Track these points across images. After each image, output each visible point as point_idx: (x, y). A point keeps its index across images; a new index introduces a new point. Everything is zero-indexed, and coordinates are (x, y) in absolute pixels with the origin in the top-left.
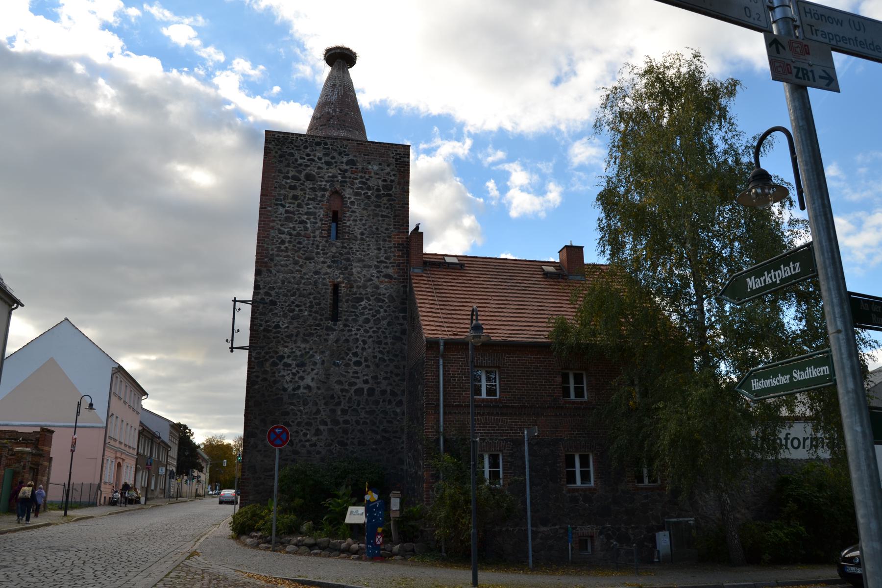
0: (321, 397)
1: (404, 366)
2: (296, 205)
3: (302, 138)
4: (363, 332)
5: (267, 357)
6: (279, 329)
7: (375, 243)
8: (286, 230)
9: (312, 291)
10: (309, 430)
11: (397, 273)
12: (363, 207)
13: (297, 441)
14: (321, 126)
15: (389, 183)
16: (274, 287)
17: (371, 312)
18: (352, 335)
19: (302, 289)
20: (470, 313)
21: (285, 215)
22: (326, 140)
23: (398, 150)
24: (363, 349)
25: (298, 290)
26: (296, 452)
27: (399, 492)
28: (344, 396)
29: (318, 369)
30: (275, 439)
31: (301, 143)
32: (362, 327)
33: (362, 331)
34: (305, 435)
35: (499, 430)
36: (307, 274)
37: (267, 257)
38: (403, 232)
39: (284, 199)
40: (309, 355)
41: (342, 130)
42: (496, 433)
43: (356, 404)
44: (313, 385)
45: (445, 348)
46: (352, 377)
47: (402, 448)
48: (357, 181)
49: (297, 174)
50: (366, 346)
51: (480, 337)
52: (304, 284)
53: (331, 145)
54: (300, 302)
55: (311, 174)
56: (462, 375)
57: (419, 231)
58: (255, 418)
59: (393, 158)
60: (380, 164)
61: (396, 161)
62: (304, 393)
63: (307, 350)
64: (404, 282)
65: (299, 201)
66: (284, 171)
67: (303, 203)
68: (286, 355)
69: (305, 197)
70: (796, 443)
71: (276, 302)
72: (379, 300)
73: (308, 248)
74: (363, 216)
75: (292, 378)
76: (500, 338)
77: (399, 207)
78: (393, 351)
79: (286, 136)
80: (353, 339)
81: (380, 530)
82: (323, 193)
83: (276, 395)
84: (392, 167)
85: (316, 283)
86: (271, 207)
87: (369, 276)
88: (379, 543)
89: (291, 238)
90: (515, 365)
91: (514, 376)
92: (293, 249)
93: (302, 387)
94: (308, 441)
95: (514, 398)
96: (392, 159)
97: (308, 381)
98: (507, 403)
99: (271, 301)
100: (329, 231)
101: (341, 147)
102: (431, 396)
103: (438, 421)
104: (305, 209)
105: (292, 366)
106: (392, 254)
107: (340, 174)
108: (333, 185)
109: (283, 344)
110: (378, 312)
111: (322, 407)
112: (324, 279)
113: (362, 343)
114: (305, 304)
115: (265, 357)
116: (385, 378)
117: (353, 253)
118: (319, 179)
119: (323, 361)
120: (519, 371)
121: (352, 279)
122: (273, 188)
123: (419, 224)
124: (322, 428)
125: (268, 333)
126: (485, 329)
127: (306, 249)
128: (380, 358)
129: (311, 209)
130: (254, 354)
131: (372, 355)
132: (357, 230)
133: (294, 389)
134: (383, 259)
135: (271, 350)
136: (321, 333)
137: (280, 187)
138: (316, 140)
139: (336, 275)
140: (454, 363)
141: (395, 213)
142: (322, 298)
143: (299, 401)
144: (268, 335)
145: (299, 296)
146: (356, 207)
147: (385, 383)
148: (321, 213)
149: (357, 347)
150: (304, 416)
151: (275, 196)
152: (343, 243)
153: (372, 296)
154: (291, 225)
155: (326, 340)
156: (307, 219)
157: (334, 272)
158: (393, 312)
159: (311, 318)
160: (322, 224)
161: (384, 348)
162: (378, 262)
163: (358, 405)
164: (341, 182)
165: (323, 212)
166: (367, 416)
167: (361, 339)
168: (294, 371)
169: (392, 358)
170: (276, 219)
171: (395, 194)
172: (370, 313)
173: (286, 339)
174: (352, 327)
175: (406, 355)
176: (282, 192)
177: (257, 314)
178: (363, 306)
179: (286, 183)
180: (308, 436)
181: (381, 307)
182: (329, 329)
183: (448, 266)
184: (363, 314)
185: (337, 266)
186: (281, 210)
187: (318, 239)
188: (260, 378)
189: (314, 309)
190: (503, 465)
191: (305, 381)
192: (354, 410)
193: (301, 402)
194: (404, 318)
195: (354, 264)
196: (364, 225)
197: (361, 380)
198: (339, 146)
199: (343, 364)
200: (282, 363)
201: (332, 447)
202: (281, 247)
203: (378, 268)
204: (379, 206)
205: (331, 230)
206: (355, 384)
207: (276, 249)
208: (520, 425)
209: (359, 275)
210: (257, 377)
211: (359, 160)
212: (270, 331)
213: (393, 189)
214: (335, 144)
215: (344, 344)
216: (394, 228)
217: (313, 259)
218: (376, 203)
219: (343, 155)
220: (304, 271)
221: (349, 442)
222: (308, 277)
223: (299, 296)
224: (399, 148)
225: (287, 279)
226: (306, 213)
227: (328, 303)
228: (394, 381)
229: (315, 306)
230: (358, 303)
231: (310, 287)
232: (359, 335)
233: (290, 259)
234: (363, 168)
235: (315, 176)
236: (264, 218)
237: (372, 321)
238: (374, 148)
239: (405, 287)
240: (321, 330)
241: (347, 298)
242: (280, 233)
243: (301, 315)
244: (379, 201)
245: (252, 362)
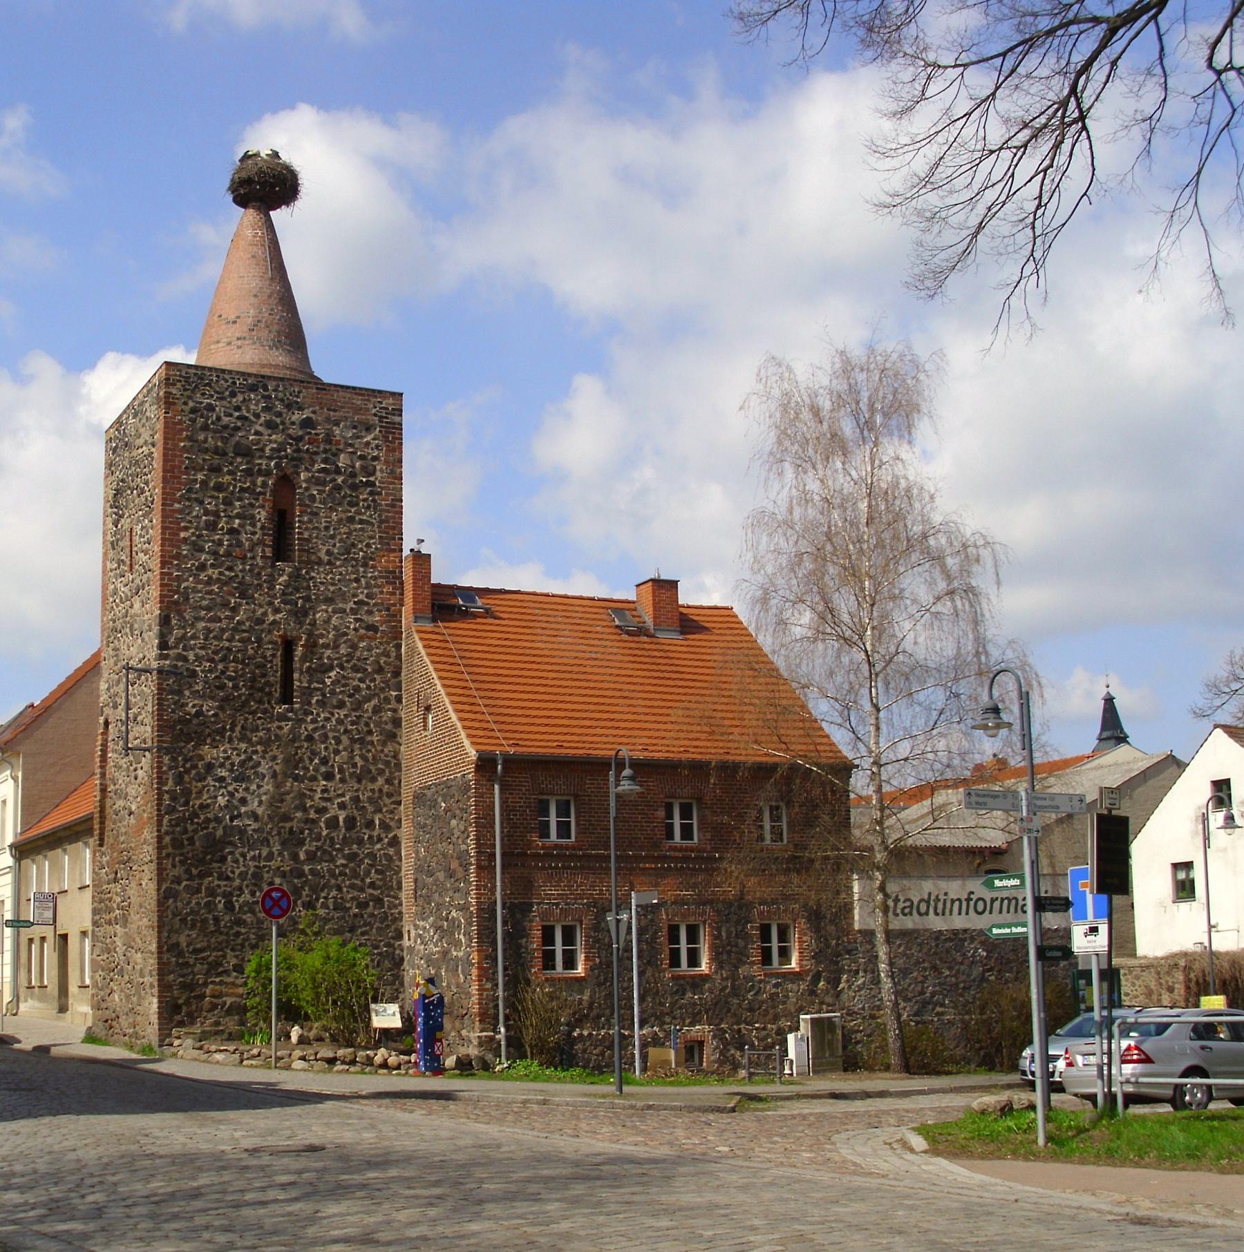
3: (227, 377)
24: (337, 752)
25: (229, 650)
37: (177, 592)
45: (504, 768)
50: (341, 748)
53: (275, 390)
59: (375, 415)
69: (235, 487)
70: (980, 906)
76: (581, 752)
77: (386, 505)
88: (438, 1053)
107: (291, 445)
141: (380, 516)
148: (262, 515)
153: (347, 661)
160: (264, 534)
162: (355, 603)
164: (293, 459)
168: (230, 788)
176: (200, 477)
179: (204, 460)
181: (362, 680)
187: (259, 561)
196: (332, 537)
203: (356, 614)
224: (385, 398)
226: (238, 516)
242: (196, 551)
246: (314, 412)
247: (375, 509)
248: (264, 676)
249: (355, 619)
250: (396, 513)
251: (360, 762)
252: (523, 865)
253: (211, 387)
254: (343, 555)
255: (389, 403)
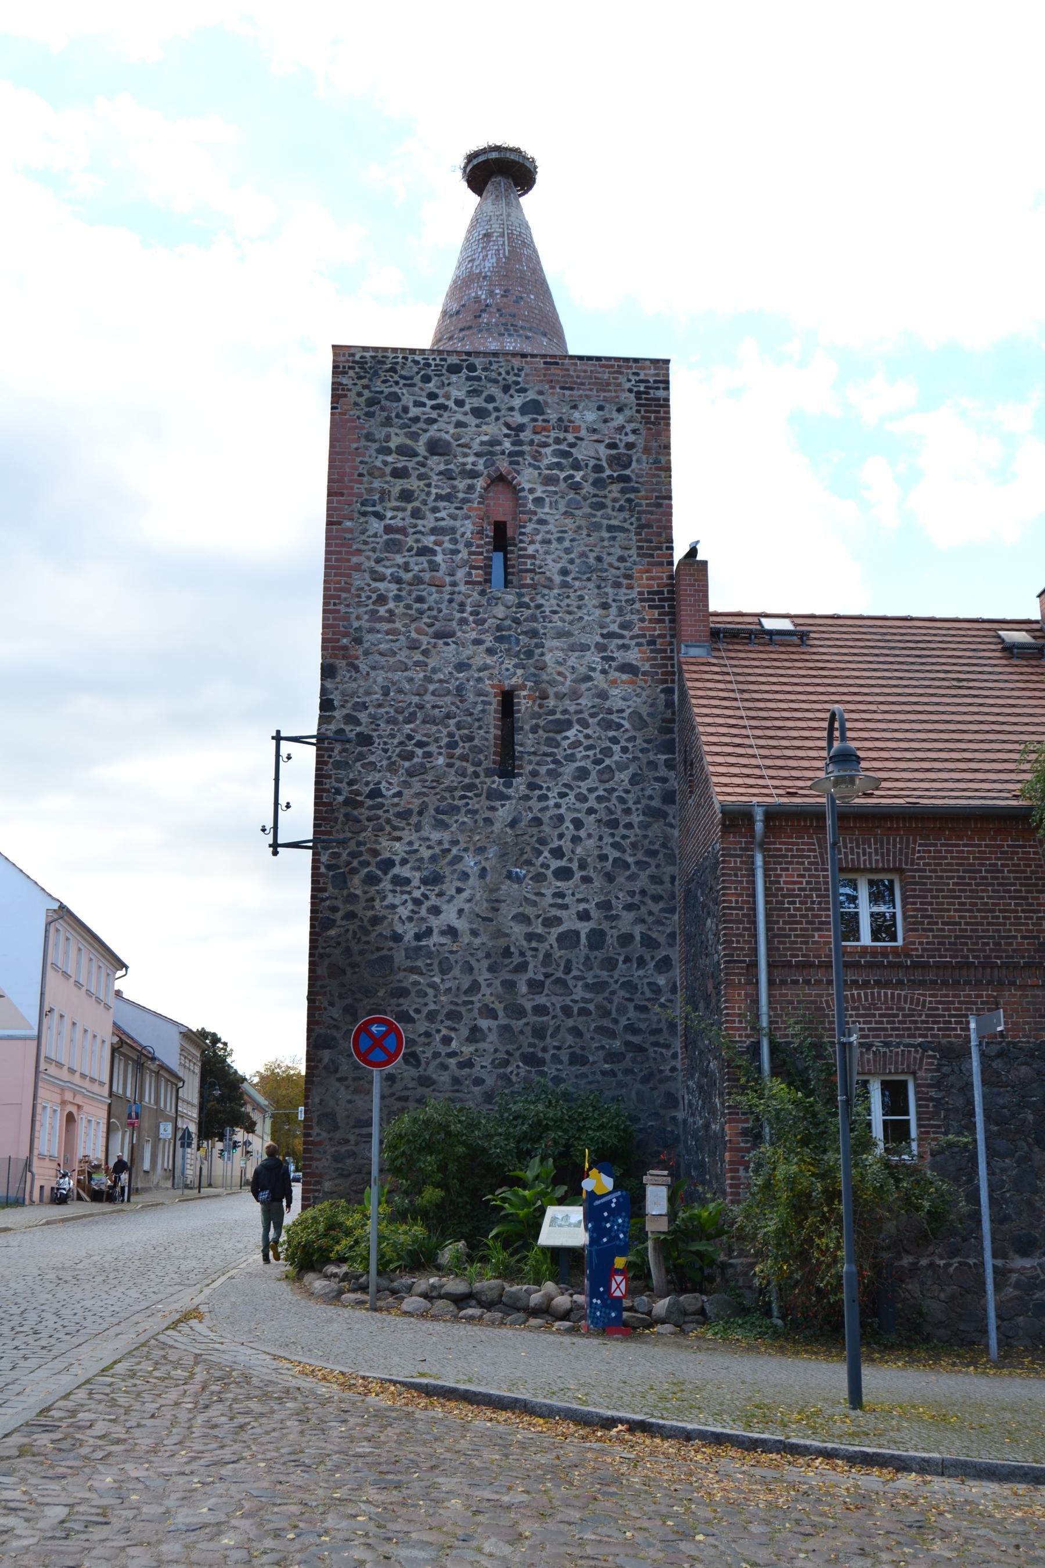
0: (480, 954)
1: (673, 879)
2: (408, 513)
3: (417, 358)
4: (573, 800)
5: (355, 864)
6: (380, 800)
7: (596, 591)
8: (388, 572)
9: (454, 708)
10: (454, 1029)
11: (648, 659)
12: (564, 509)
13: (429, 1055)
14: (462, 330)
15: (622, 450)
16: (364, 703)
17: (591, 753)
18: (547, 808)
19: (428, 706)
20: (825, 724)
21: (386, 537)
22: (472, 359)
23: (642, 373)
24: (576, 840)
25: (421, 707)
26: (426, 1082)
27: (666, 1173)
28: (535, 949)
29: (473, 888)
30: (370, 1050)
31: (415, 369)
32: (571, 788)
33: (571, 796)
34: (447, 1041)
35: (904, 1022)
36: (440, 670)
37: (346, 635)
38: (661, 564)
39: (382, 500)
40: (449, 857)
41: (510, 335)
42: (897, 1029)
43: (562, 968)
44: (461, 925)
45: (767, 827)
46: (551, 905)
47: (673, 1069)
48: (548, 450)
49: (408, 442)
50: (582, 833)
51: (851, 780)
52: (433, 694)
53: (484, 369)
54: (425, 735)
55: (440, 440)
56: (811, 890)
57: (699, 558)
58: (332, 1004)
59: (630, 391)
60: (600, 408)
61: (638, 399)
62: (442, 945)
63: (446, 846)
64: (665, 681)
65: (416, 504)
66: (377, 437)
67: (423, 508)
68: (397, 859)
69: (428, 494)
71: (371, 737)
72: (607, 725)
73: (440, 611)
74: (565, 532)
75: (413, 911)
77: (648, 505)
78: (646, 842)
79: (380, 355)
80: (551, 818)
81: (620, 1262)
82: (469, 481)
83: (379, 949)
84: (627, 412)
85: (460, 690)
86: (352, 519)
87: (583, 670)
88: (618, 1293)
89: (399, 590)
90: (940, 864)
91: (937, 890)
92: (405, 614)
93: (436, 931)
94: (452, 1054)
95: (939, 943)
96: (627, 394)
97: (449, 916)
98: (922, 956)
99: (358, 735)
100: (487, 569)
101: (508, 373)
102: (738, 942)
103: (756, 1001)
104: (429, 522)
105: (412, 885)
106: (635, 617)
107: (506, 436)
108: (493, 465)
109: (390, 834)
110: (607, 752)
111: (483, 976)
112: (480, 680)
113: (571, 827)
114: (437, 740)
115: (349, 863)
116: (629, 907)
117: (544, 618)
118: (459, 449)
119: (484, 869)
120: (952, 878)
121: (545, 677)
122: (356, 477)
123: (698, 542)
124: (484, 1023)
125: (355, 808)
126: (864, 759)
127: (435, 613)
128: (615, 860)
129: (443, 519)
130: (324, 858)
131: (596, 853)
132: (551, 564)
133: (418, 937)
134: (614, 628)
135: (362, 848)
136: (477, 806)
137: (370, 474)
138: (449, 361)
139: (508, 670)
140: (791, 863)
141: (639, 519)
142: (477, 724)
143: (431, 965)
144: (356, 813)
145: (424, 722)
146: (547, 510)
147: (628, 917)
148: (467, 528)
149: (561, 836)
150: (443, 998)
151: (360, 495)
152: (520, 595)
153: (592, 715)
154: (400, 560)
155: (488, 821)
156: (436, 543)
157: (502, 663)
158: (642, 751)
159: (452, 771)
160: (471, 553)
161: (624, 837)
162: (603, 636)
163: (568, 970)
164: (511, 454)
165: (471, 527)
166: (588, 996)
167: (569, 817)
168: (417, 894)
169: (645, 859)
170: (363, 547)
171: (638, 476)
172: (588, 756)
173: (397, 822)
174: (549, 789)
175: (677, 852)
176: (377, 484)
177: (330, 766)
178: (572, 739)
179: (385, 463)
180: (454, 1044)
181: (614, 740)
182: (494, 795)
183: (771, 640)
184: (571, 758)
185: (508, 650)
186: (376, 526)
187: (462, 588)
188: (340, 914)
189: (458, 751)
190: (918, 1106)
191: (442, 916)
192: (559, 981)
193: (436, 966)
194: (670, 765)
195: (549, 643)
196: (568, 551)
197: (573, 911)
198: (502, 370)
199: (530, 875)
200: (389, 876)
201: (509, 1069)
202: (377, 611)
204: (602, 506)
205: (490, 566)
206: (558, 921)
207: (366, 617)
208: (955, 1009)
209: (561, 669)
210: (334, 909)
211: (549, 401)
212: (361, 804)
213: (634, 464)
214: (494, 367)
215: (529, 830)
216: (639, 555)
217: (452, 634)
218: (594, 500)
219: (512, 392)
220: (432, 663)
221: (547, 1057)
222: (442, 677)
223: (424, 722)
225: (394, 684)
226: (434, 531)
227: (491, 736)
228: (650, 913)
229: (461, 744)
230: (559, 732)
231: (448, 699)
232: (564, 807)
233: (401, 637)
234: (560, 420)
235: (449, 443)
236: (337, 545)
237: (594, 774)
238: (585, 371)
239: (669, 691)
240: (475, 799)
241: (534, 721)
242: (375, 580)
243: (428, 765)
244: (601, 493)
245: (321, 875)
246: (541, 393)
247: (631, 510)
248: (471, 739)
249: (603, 658)
250: (662, 514)
251: (615, 854)
252: (807, 982)
253: (396, 372)
254: (585, 573)
255: (650, 372)
